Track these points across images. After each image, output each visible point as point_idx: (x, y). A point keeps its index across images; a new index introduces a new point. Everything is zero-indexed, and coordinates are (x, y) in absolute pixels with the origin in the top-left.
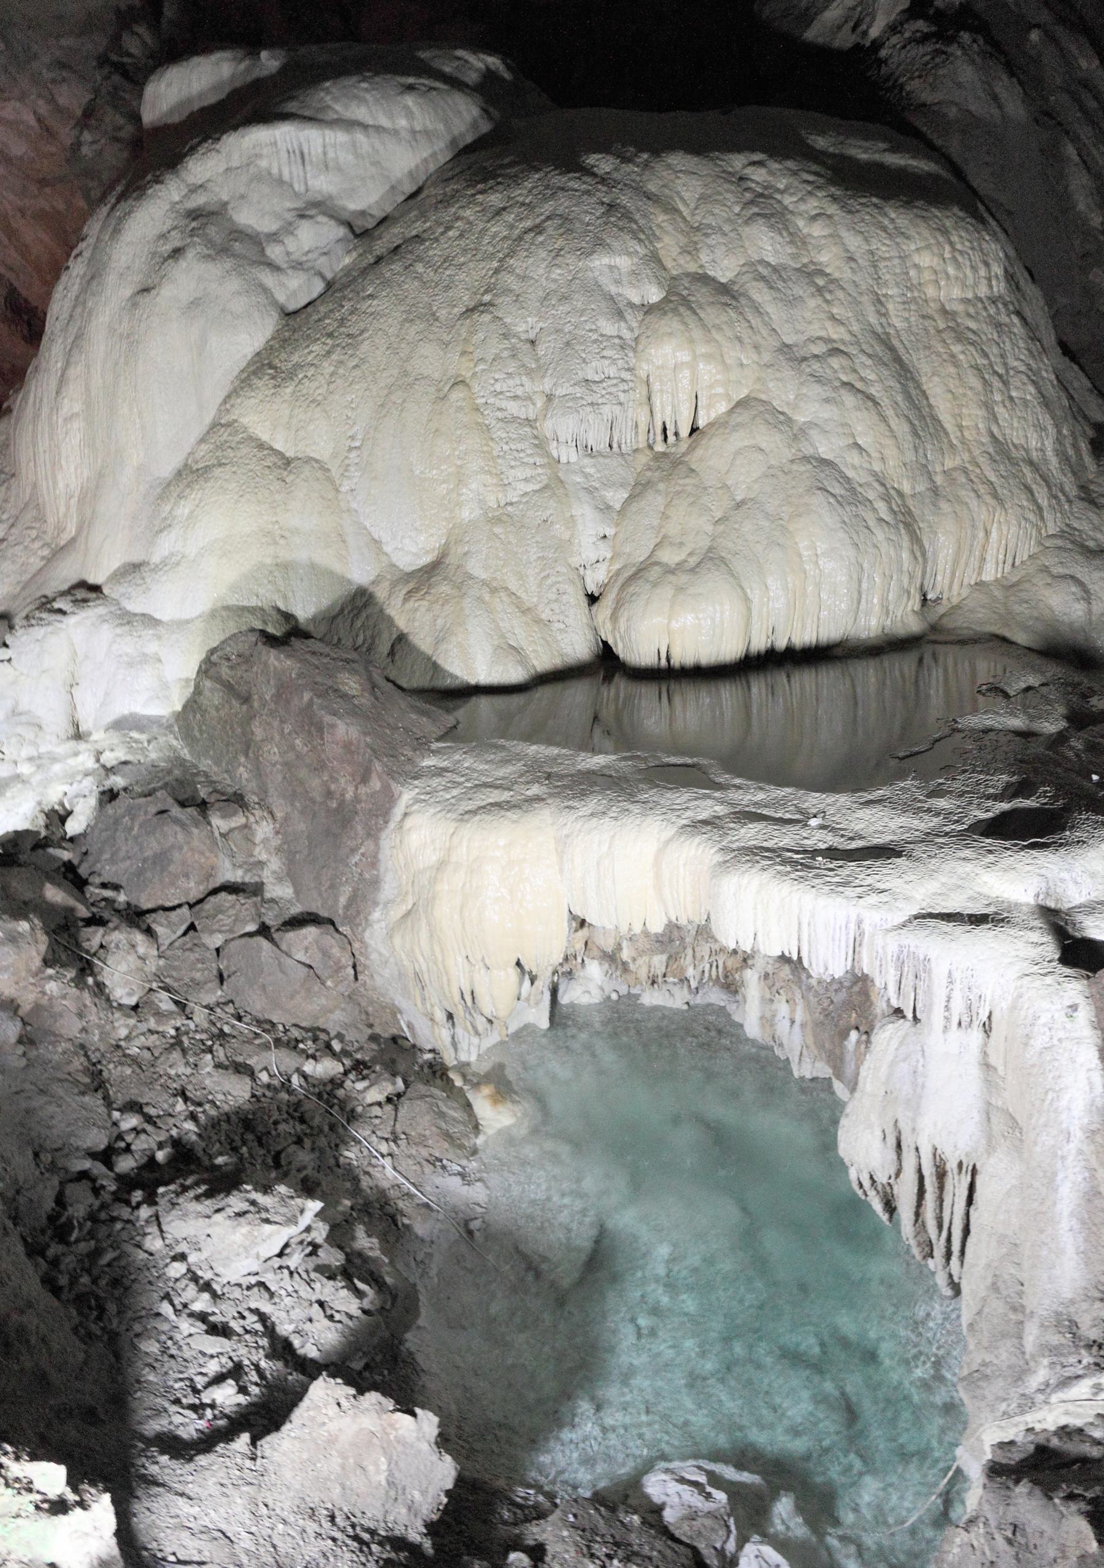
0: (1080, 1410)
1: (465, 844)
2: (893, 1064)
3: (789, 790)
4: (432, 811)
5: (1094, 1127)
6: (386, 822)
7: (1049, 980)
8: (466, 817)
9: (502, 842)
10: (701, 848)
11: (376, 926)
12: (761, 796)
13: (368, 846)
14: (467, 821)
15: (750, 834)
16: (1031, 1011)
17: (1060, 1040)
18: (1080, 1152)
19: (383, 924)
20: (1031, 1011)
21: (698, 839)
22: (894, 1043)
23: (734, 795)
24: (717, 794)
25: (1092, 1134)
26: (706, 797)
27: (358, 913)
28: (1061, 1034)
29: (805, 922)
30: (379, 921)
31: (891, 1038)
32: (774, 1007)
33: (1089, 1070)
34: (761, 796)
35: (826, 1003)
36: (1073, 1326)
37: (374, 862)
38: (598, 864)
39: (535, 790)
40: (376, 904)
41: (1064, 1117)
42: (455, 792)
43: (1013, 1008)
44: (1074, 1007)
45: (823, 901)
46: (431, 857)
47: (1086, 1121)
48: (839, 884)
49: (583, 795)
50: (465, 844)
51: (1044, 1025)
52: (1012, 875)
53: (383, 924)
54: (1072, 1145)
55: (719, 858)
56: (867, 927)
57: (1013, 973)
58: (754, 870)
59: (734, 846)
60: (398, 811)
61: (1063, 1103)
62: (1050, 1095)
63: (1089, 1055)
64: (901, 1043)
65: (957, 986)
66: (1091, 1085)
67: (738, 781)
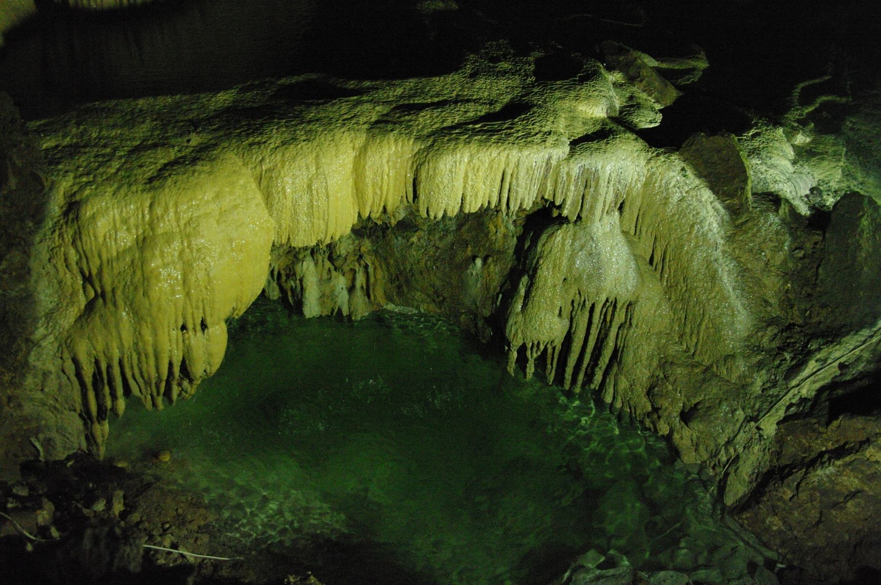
0: (821, 376)
1: (172, 211)
2: (572, 259)
3: (411, 83)
4: (110, 190)
5: (729, 234)
6: (39, 222)
7: (662, 158)
8: (156, 183)
9: (209, 196)
10: (400, 144)
11: (44, 344)
12: (399, 91)
13: (16, 256)
14: (162, 187)
15: (426, 120)
16: (664, 181)
17: (686, 192)
18: (724, 252)
19: (51, 338)
20: (664, 181)
21: (392, 136)
22: (569, 241)
23: (380, 95)
24: (365, 98)
25: (730, 239)
26: (358, 103)
27: (13, 339)
28: (686, 189)
29: (509, 172)
30: (45, 337)
31: (564, 240)
32: (332, 284)
33: (711, 203)
34: (399, 91)
35: (432, 251)
36: (759, 349)
37: (23, 273)
38: (309, 187)
39: (195, 140)
40: (36, 320)
41: (710, 235)
42: (116, 164)
43: (646, 185)
44: (683, 169)
45: (526, 152)
46: (126, 239)
47: (723, 232)
48: (523, 136)
49: (258, 130)
50: (172, 211)
51: (674, 186)
52: (592, 100)
53: (51, 338)
54: (718, 250)
55: (419, 146)
56: (554, 162)
57: (643, 162)
58: (461, 146)
59: (425, 132)
60: (56, 205)
61: (706, 228)
62: (696, 228)
63: (707, 195)
64: (574, 240)
65: (612, 183)
66: (716, 210)
67: (367, 84)
